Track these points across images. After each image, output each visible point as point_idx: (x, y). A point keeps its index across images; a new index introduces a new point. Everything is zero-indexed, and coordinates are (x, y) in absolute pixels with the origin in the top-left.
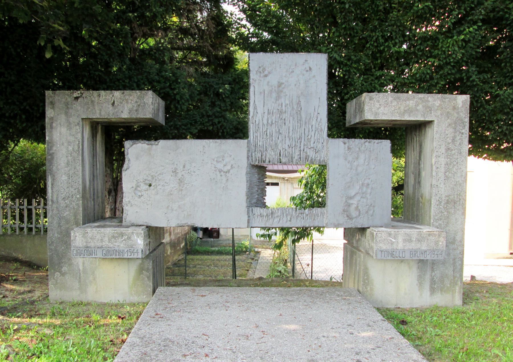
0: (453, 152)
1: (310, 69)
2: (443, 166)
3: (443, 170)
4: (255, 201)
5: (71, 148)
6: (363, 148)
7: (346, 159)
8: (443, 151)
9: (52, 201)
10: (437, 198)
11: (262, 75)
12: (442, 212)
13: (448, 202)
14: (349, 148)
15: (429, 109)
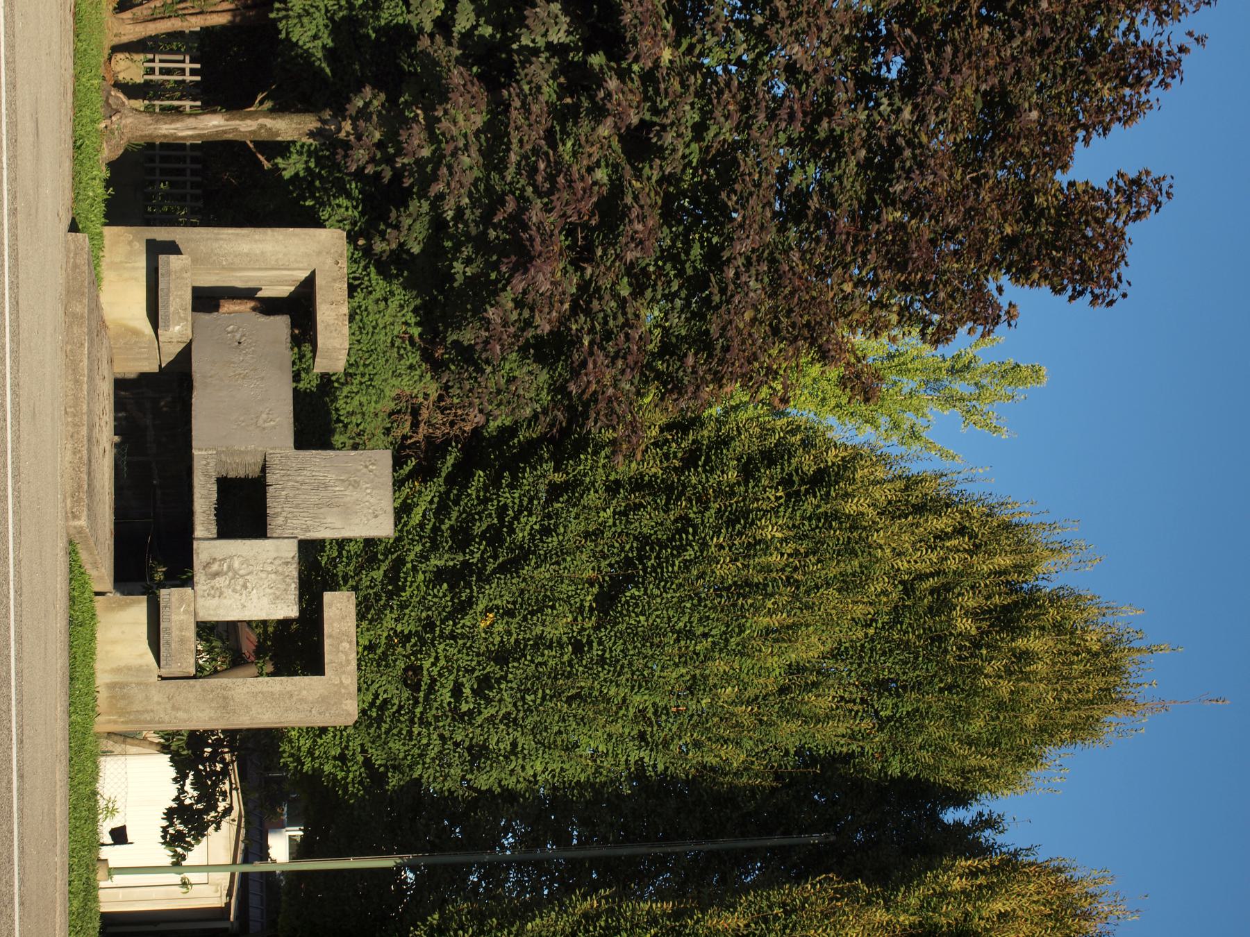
0: (288, 701)
1: (376, 516)
2: (270, 689)
3: (265, 689)
4: (224, 459)
5: (281, 256)
6: (287, 580)
7: (275, 559)
8: (288, 689)
9: (218, 234)
10: (230, 685)
11: (368, 463)
12: (212, 691)
13: (225, 698)
14: (287, 563)
15: (340, 669)
